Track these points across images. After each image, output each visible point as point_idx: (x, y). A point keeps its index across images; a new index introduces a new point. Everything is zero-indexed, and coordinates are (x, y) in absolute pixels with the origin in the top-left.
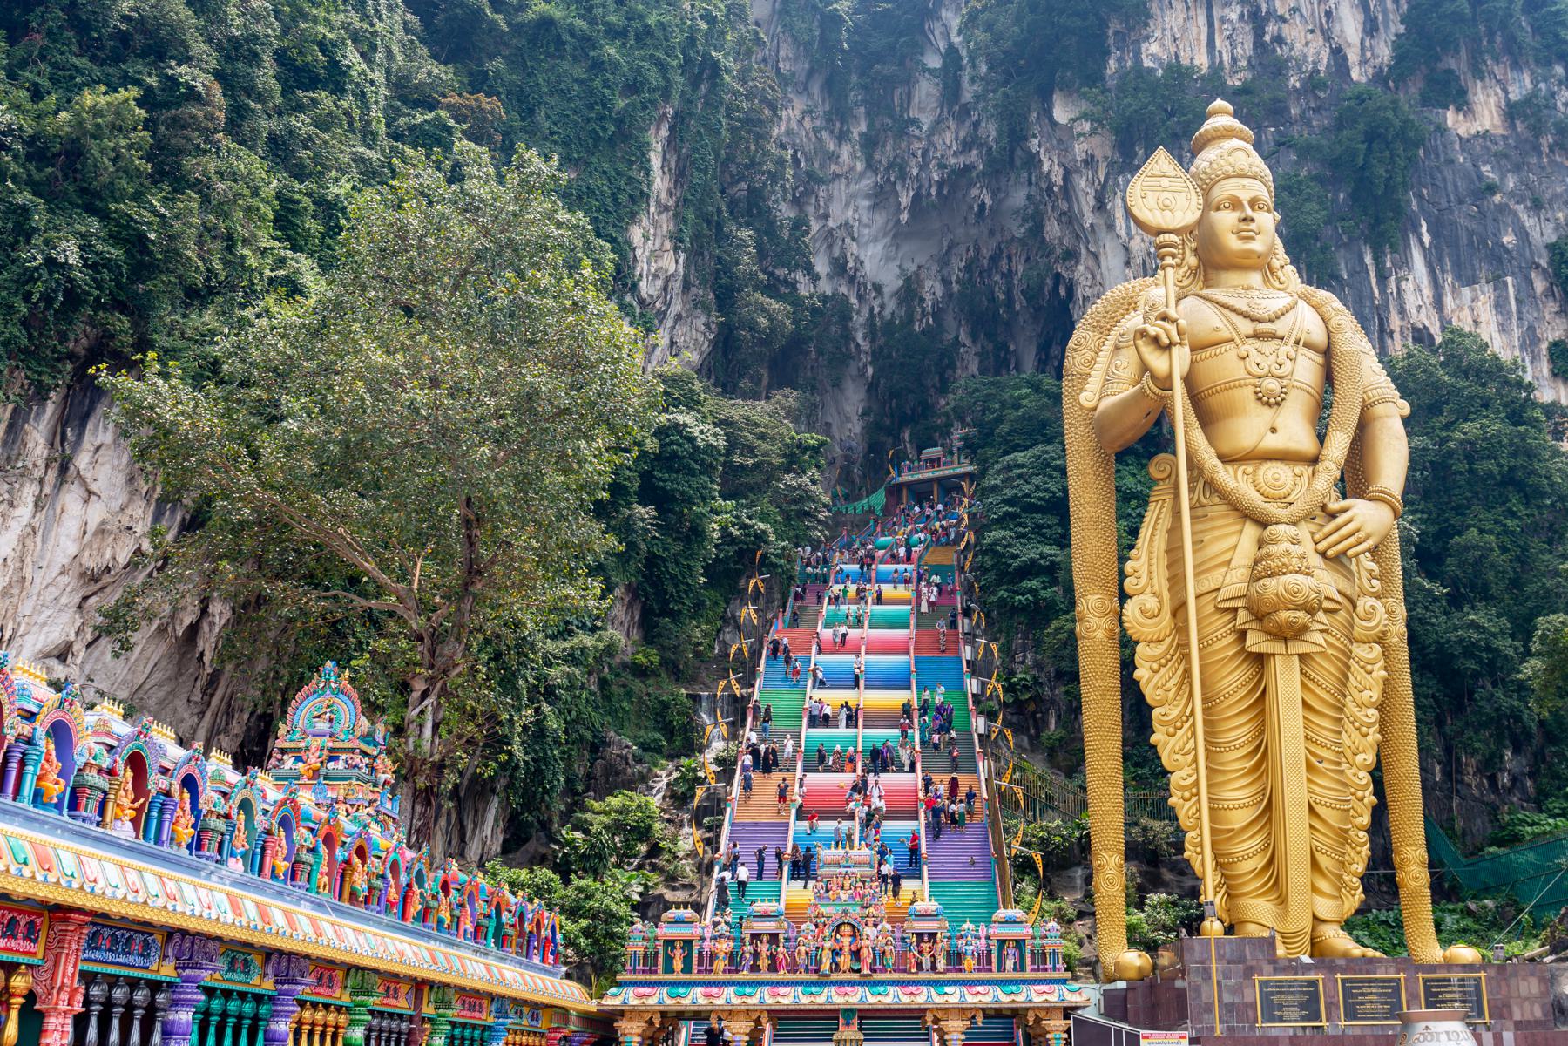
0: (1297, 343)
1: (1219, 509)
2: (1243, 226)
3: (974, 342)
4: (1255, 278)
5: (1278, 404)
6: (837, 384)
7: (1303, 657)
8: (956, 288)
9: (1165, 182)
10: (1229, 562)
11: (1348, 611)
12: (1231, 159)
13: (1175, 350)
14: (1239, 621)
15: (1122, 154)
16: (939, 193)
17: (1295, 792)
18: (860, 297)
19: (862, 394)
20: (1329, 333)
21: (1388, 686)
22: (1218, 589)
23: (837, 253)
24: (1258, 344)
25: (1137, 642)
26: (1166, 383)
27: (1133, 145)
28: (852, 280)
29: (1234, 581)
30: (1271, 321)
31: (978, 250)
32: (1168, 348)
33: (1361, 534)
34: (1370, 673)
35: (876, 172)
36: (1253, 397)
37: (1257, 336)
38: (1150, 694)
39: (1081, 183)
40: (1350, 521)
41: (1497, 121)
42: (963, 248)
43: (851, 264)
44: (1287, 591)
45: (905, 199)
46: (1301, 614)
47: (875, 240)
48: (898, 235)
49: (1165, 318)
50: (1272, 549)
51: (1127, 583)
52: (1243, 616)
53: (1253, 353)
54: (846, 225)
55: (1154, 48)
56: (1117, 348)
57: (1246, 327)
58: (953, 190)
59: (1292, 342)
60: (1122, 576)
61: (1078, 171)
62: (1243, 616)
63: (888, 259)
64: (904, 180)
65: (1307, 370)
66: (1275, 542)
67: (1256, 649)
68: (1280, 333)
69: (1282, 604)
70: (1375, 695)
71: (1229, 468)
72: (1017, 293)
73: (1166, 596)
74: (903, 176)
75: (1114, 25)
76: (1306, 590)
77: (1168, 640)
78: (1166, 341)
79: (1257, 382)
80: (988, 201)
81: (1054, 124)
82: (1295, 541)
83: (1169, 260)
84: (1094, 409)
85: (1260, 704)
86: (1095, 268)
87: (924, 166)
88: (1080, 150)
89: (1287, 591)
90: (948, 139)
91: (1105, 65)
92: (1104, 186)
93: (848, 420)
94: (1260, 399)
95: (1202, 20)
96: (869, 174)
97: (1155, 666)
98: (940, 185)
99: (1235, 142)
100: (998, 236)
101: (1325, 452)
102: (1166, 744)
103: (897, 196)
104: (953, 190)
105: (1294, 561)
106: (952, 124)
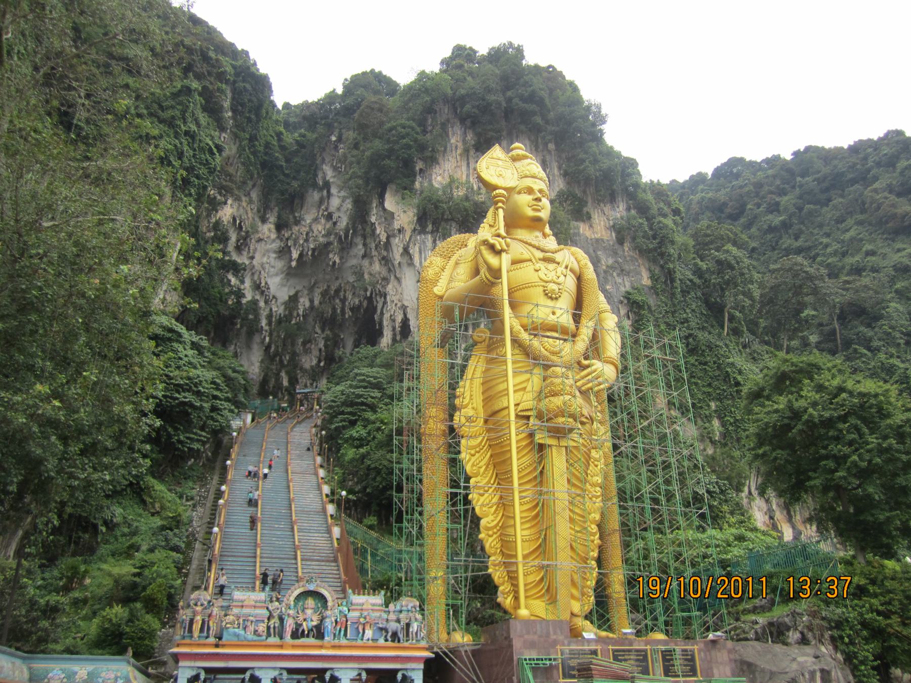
0: (566, 267)
3: (323, 331)
5: (556, 299)
6: (249, 347)
8: (316, 302)
9: (500, 163)
10: (525, 388)
12: (528, 168)
13: (504, 255)
15: (420, 225)
16: (313, 255)
17: (563, 531)
18: (266, 302)
19: (262, 353)
20: (580, 268)
23: (256, 277)
24: (546, 264)
27: (426, 222)
28: (262, 293)
30: (553, 253)
31: (329, 287)
32: (498, 253)
33: (600, 380)
34: (596, 466)
35: (281, 240)
36: (542, 294)
37: (545, 260)
38: (468, 468)
39: (396, 241)
40: (595, 371)
41: (604, 233)
42: (321, 285)
43: (263, 284)
45: (295, 255)
46: (571, 420)
47: (277, 275)
48: (290, 273)
51: (457, 402)
53: (543, 268)
54: (262, 265)
55: (439, 178)
56: (457, 264)
57: (540, 255)
58: (320, 254)
59: (564, 266)
60: (452, 397)
61: (394, 236)
63: (283, 285)
64: (295, 245)
65: (570, 283)
69: (562, 413)
72: (347, 310)
73: (481, 410)
74: (296, 241)
75: (419, 165)
77: (481, 438)
78: (498, 247)
79: (544, 284)
80: (338, 261)
81: (384, 209)
83: (500, 204)
84: (441, 297)
85: (540, 477)
86: (398, 287)
87: (306, 240)
88: (396, 225)
90: (320, 228)
91: (413, 182)
92: (408, 243)
93: (253, 364)
94: (546, 294)
95: (464, 168)
96: (278, 241)
97: (473, 452)
98: (314, 250)
99: (529, 161)
100: (340, 281)
102: (478, 500)
103: (290, 252)
104: (320, 254)
105: (568, 388)
106: (323, 221)
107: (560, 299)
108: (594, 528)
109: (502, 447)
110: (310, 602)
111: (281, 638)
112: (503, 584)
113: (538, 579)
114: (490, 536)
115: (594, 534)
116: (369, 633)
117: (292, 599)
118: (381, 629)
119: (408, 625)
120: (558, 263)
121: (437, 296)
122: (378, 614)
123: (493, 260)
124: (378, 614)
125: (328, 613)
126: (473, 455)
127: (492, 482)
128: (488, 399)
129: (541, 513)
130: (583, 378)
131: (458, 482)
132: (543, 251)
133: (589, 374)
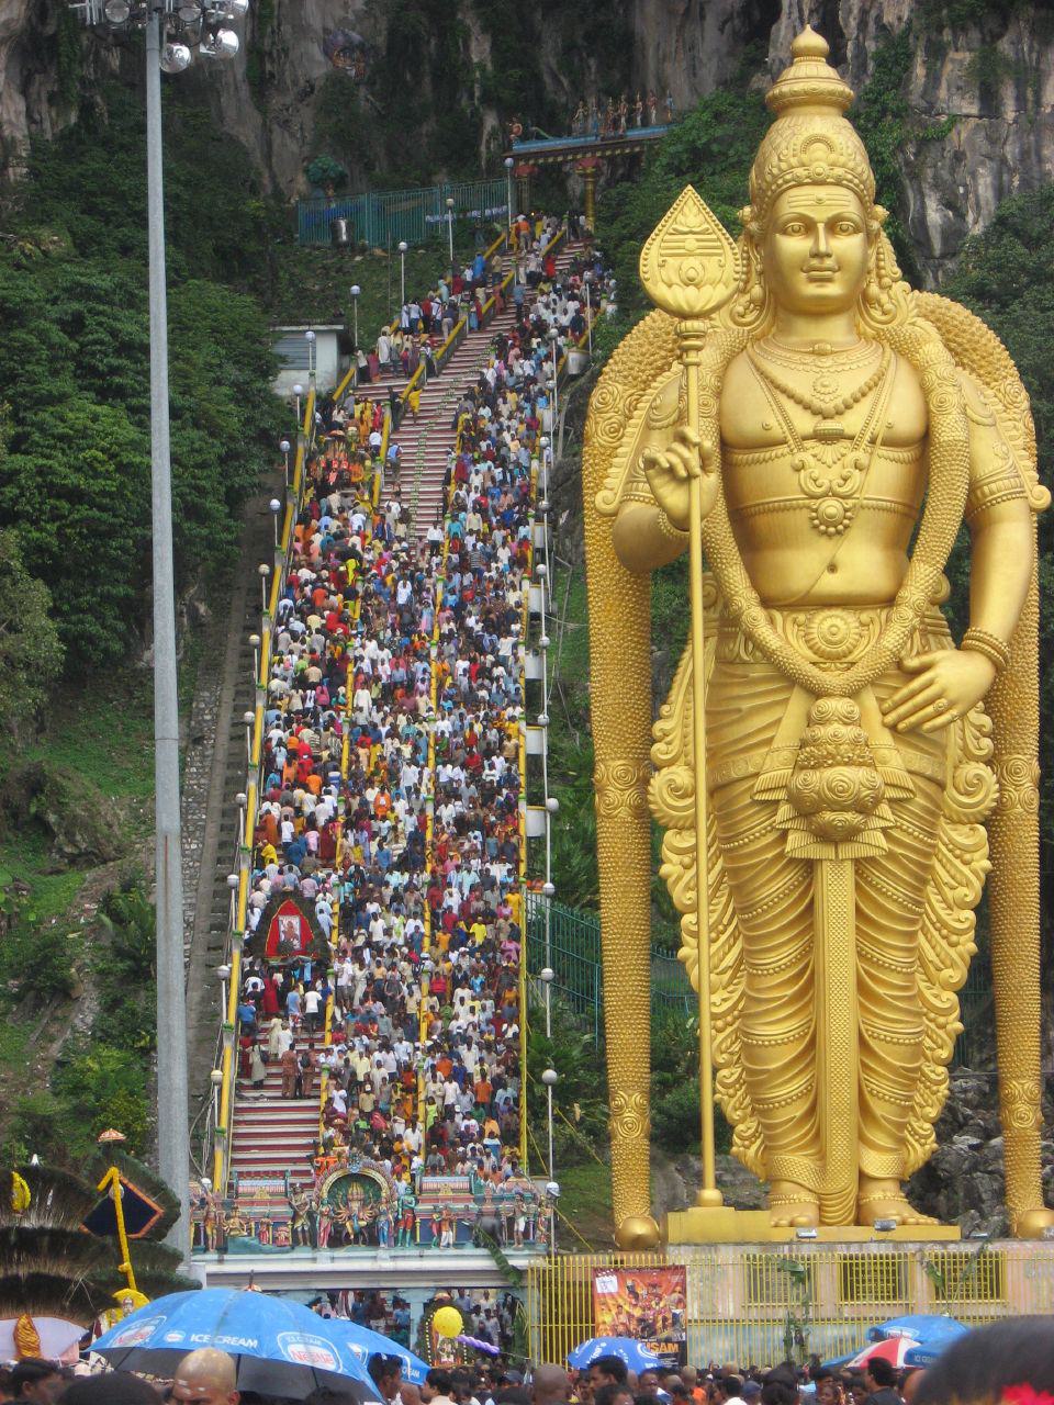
0: (873, 441)
1: (758, 672)
2: (815, 262)
4: (835, 330)
5: (839, 533)
7: (857, 862)
9: (691, 242)
10: (769, 741)
11: (927, 796)
13: (695, 484)
14: (778, 818)
20: (928, 415)
21: (990, 884)
22: (757, 775)
25: (666, 828)
26: (682, 523)
29: (772, 768)
30: (839, 413)
33: (943, 702)
36: (806, 526)
38: (680, 896)
44: (830, 789)
49: (683, 440)
50: (822, 732)
52: (784, 811)
57: (805, 423)
62: (784, 811)
65: (884, 477)
66: (823, 721)
67: (797, 855)
68: (848, 431)
70: (972, 894)
71: (778, 616)
76: (854, 788)
78: (683, 473)
79: (814, 503)
82: (847, 720)
84: (615, 514)
89: (830, 789)
94: (816, 527)
97: (687, 860)
101: (902, 593)
107: (854, 533)
108: (949, 999)
109: (733, 859)
110: (356, 1190)
111: (314, 1246)
112: (742, 1120)
113: (798, 1114)
114: (719, 1031)
115: (945, 1012)
116: (448, 1236)
117: (325, 1188)
118: (470, 1228)
119: (512, 1221)
120: (851, 438)
121: (605, 515)
122: (461, 1206)
123: (674, 497)
124: (461, 1206)
125: (383, 1207)
126: (687, 867)
127: (725, 921)
128: (712, 754)
129: (808, 985)
130: (897, 706)
131: (663, 914)
132: (815, 413)
133: (913, 695)
